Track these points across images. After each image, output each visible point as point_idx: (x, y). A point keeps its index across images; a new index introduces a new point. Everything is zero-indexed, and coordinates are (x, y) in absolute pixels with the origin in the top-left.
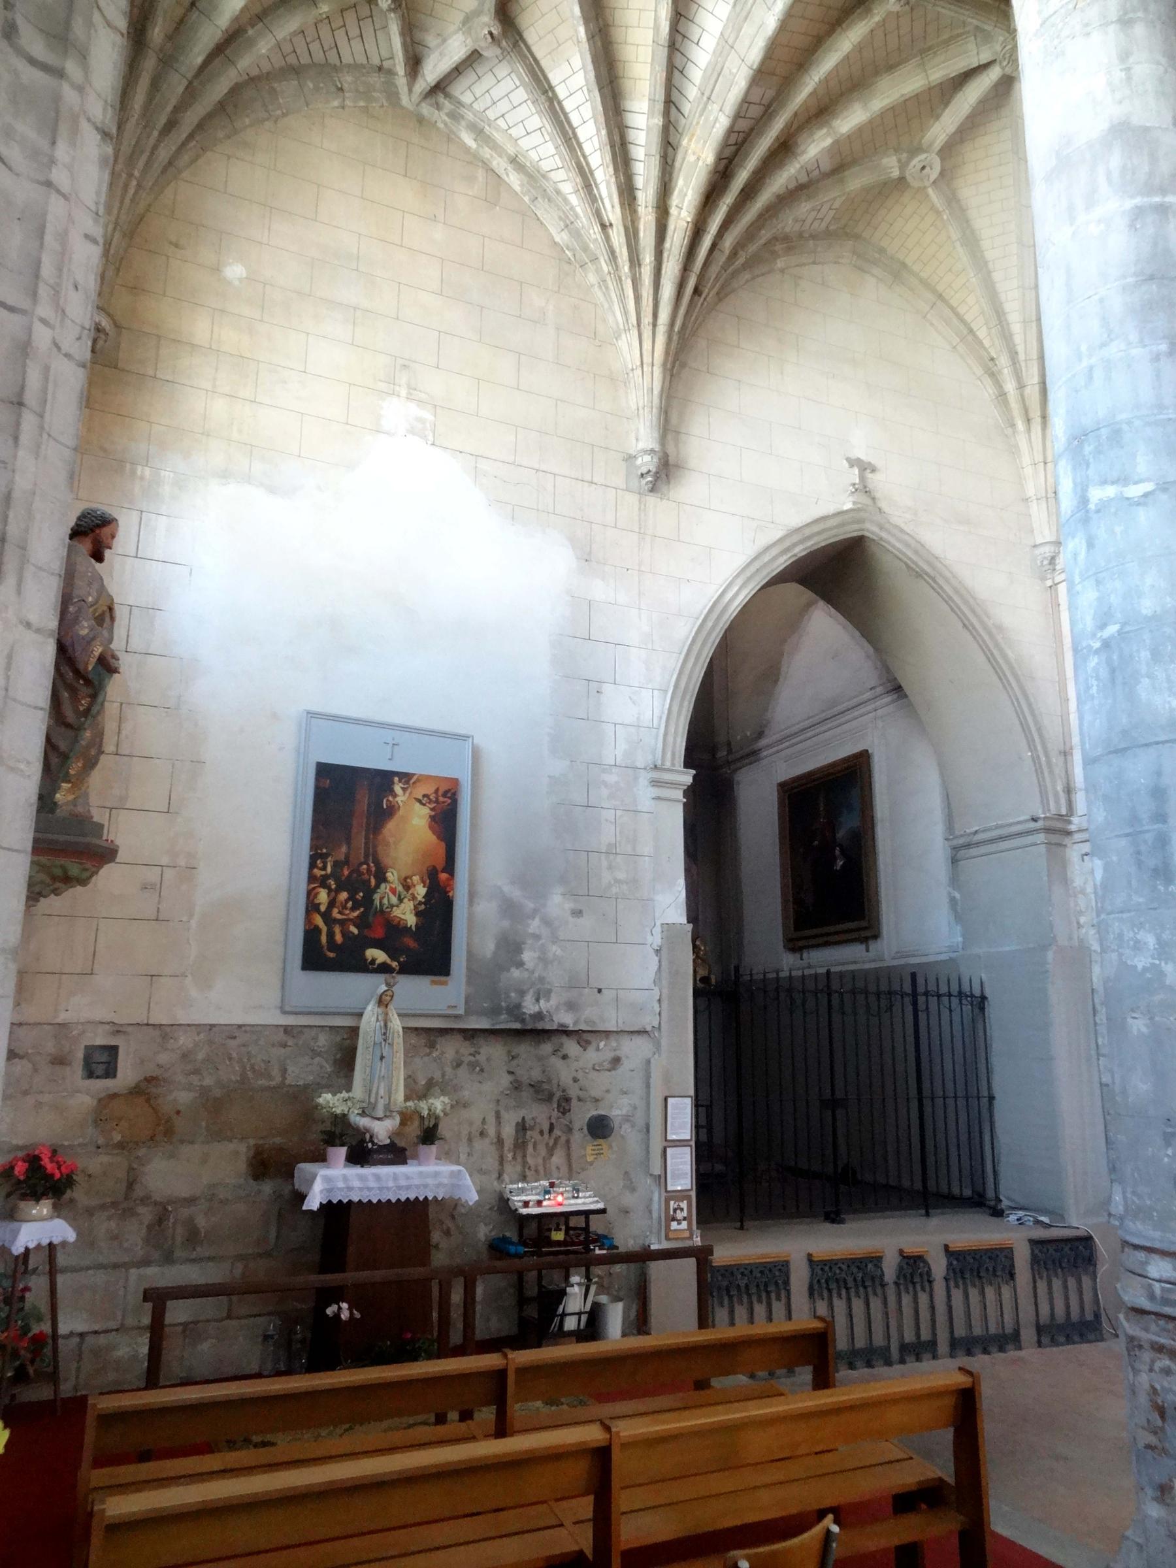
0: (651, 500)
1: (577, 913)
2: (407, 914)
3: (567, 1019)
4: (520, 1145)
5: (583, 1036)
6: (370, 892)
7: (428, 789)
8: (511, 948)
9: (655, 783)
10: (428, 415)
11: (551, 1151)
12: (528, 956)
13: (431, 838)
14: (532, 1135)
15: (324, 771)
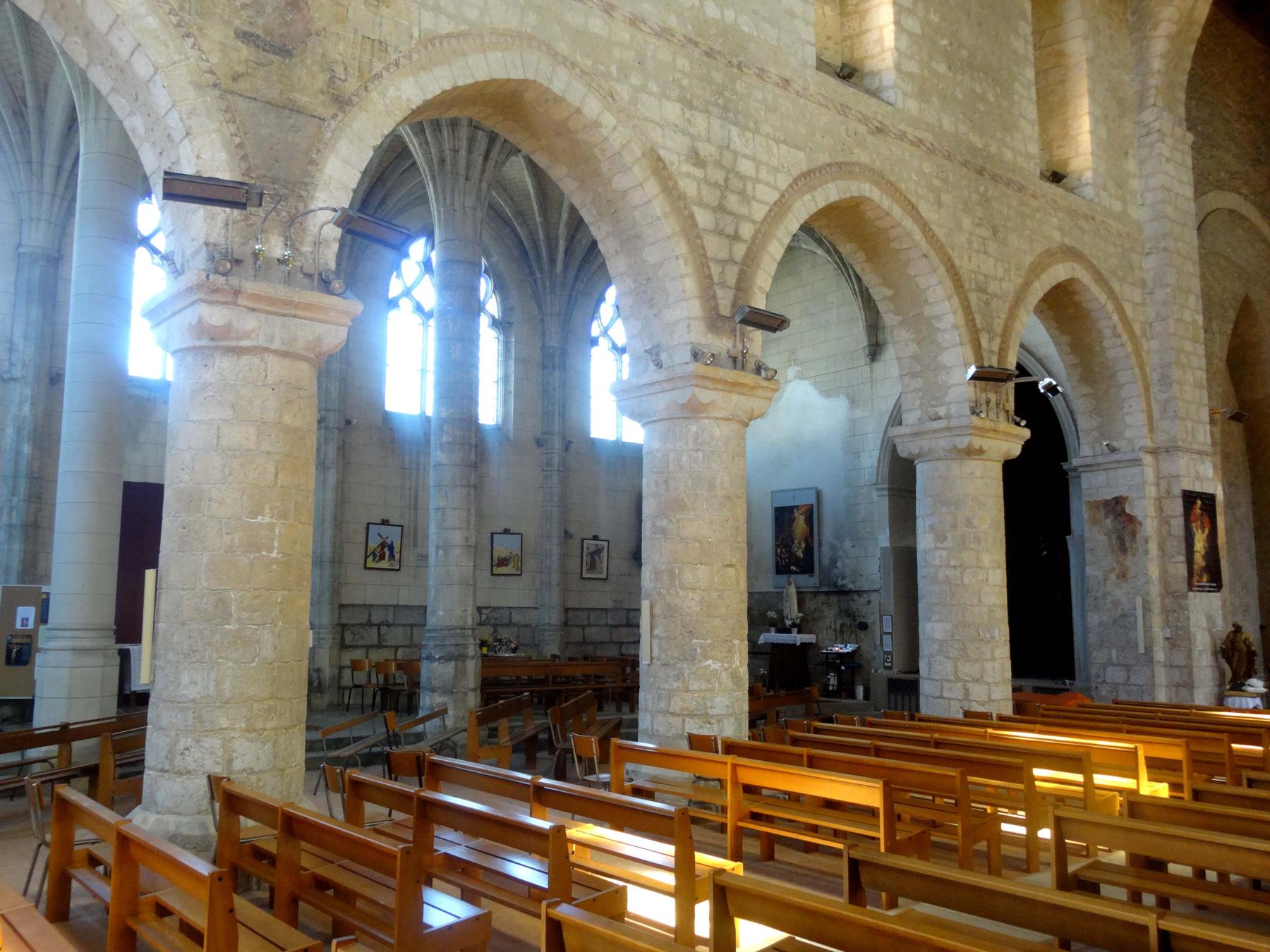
0: (876, 365)
1: (853, 547)
2: (800, 554)
3: (851, 586)
4: (842, 631)
5: (859, 593)
6: (790, 547)
7: (803, 510)
8: (834, 562)
9: (878, 490)
10: (799, 368)
11: (851, 633)
12: (839, 564)
13: (805, 526)
14: (845, 629)
15: (777, 509)
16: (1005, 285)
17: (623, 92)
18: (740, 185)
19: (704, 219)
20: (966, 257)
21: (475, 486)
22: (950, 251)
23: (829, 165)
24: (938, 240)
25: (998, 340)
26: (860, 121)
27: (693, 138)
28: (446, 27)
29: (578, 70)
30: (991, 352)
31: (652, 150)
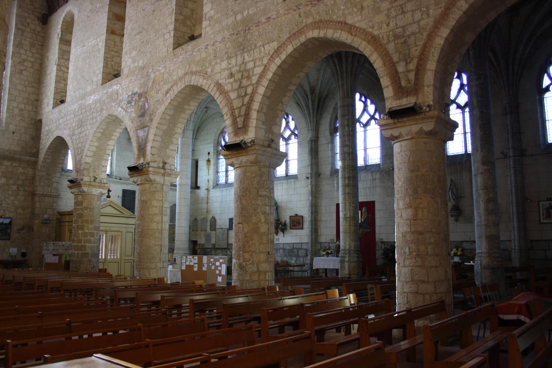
16: (422, 23)
17: (209, 70)
18: (248, 74)
19: (233, 95)
20: (385, 26)
21: (348, 193)
22: (370, 30)
23: (289, 38)
24: (361, 29)
25: (415, 61)
26: (307, 5)
27: (230, 69)
28: (170, 85)
29: (198, 73)
30: (409, 71)
31: (218, 82)
